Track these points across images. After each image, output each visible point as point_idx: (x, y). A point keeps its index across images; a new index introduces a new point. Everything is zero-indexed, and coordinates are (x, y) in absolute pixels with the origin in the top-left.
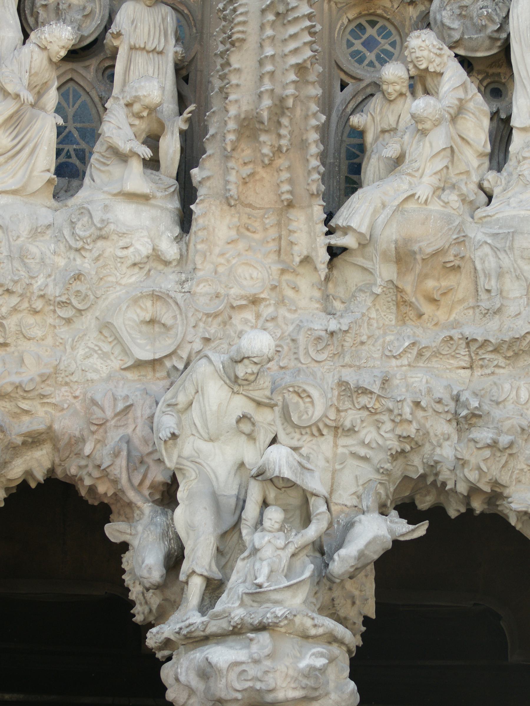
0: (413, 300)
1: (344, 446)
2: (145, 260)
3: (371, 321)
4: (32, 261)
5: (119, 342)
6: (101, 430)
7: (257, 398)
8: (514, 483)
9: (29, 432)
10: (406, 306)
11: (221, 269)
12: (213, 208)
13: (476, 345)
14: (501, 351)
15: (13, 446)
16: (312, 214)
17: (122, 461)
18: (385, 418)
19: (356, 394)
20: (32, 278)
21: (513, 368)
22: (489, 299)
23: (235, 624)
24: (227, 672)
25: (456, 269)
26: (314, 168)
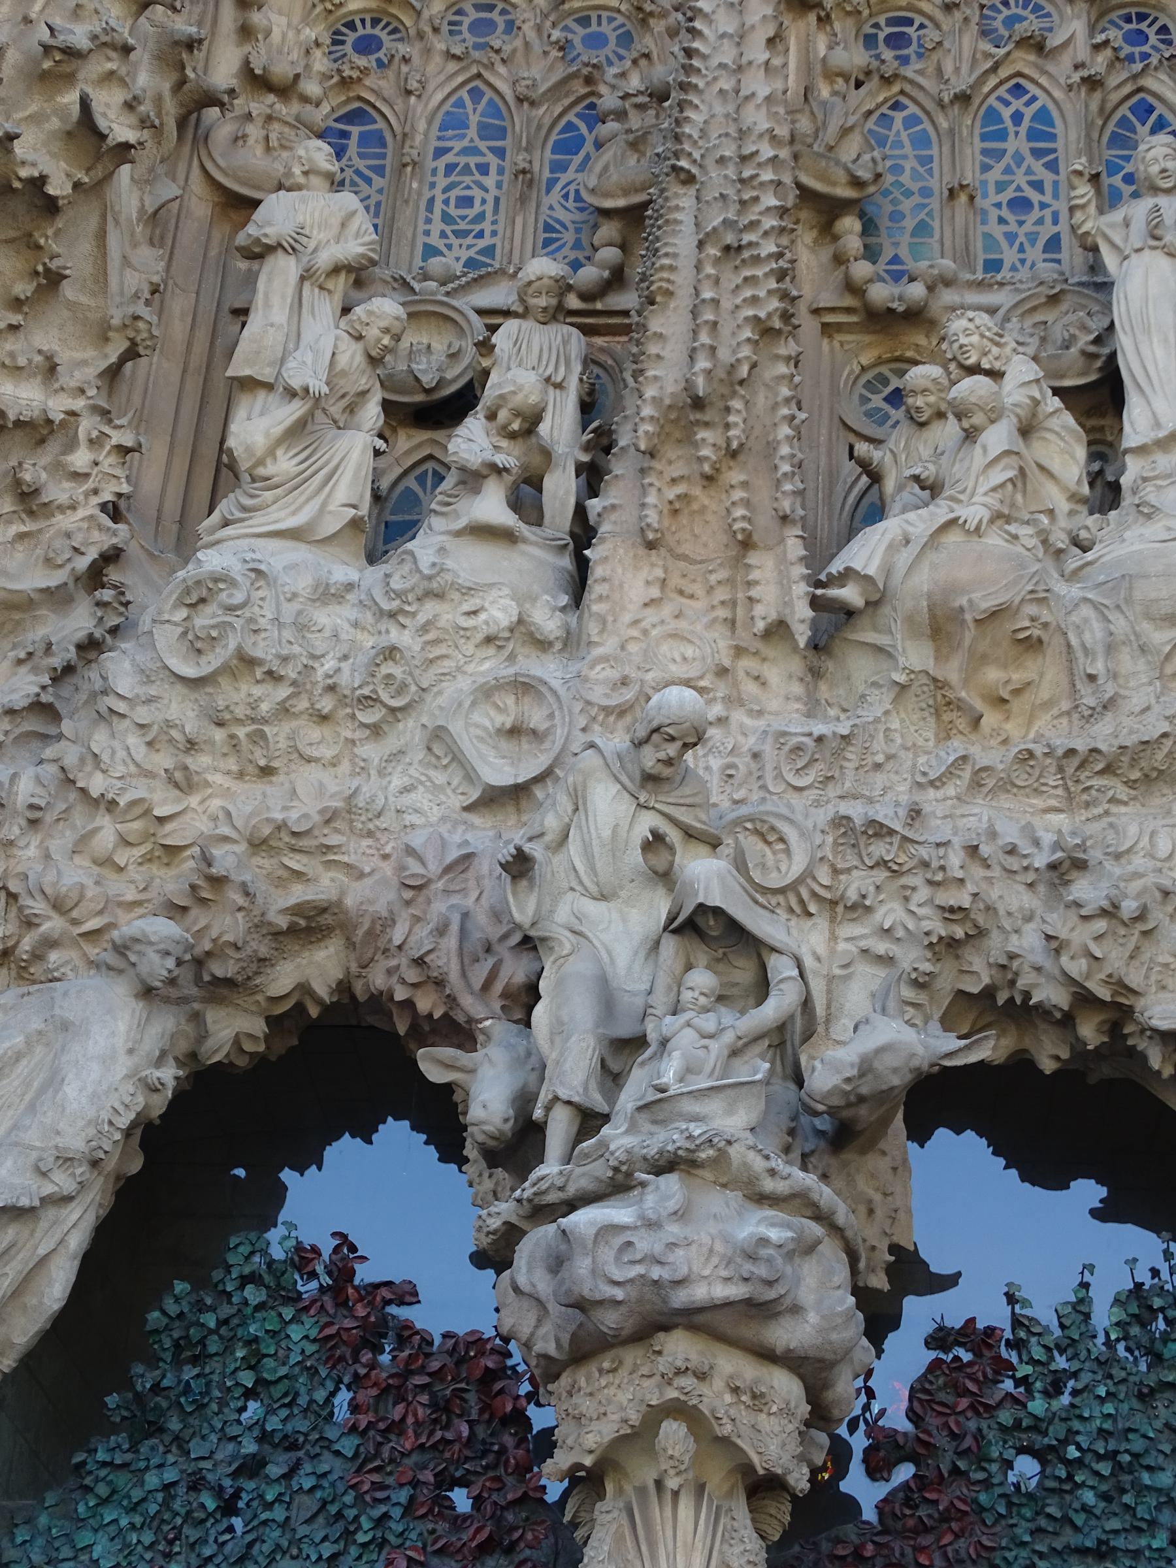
0: (963, 694)
1: (848, 940)
2: (507, 634)
5: (462, 765)
6: (421, 899)
7: (682, 818)
8: (1153, 989)
9: (298, 905)
11: (633, 648)
13: (1075, 762)
15: (273, 930)
16: (785, 552)
17: (451, 942)
20: (314, 657)
23: (615, 1163)
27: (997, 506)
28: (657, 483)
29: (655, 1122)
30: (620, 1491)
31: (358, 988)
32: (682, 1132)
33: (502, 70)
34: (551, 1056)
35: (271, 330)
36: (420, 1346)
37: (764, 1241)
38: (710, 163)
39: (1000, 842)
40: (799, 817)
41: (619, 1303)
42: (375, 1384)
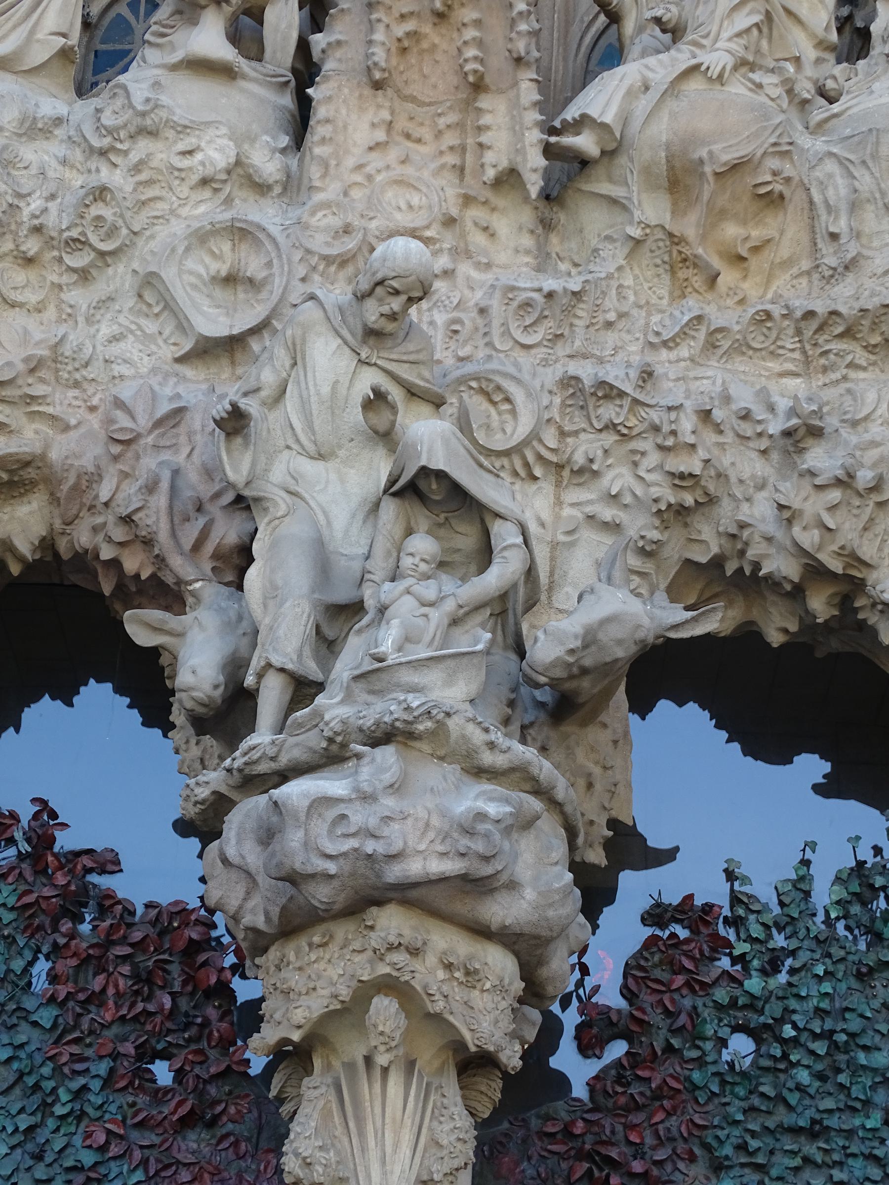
0: (700, 251)
1: (573, 505)
2: (224, 177)
3: (625, 290)
4: (24, 172)
6: (130, 455)
10: (688, 268)
12: (346, 91)
13: (814, 324)
14: (858, 336)
16: (518, 96)
17: (161, 500)
18: (646, 444)
19: (594, 398)
20: (20, 196)
21: (883, 371)
22: (835, 253)
23: (330, 734)
24: (307, 817)
27: (741, 52)
28: (385, 19)
29: (372, 692)
30: (328, 1067)
31: (62, 545)
32: (400, 703)
34: (264, 623)
36: (122, 916)
37: (481, 816)
39: (734, 407)
40: (526, 377)
41: (331, 877)
42: (75, 954)
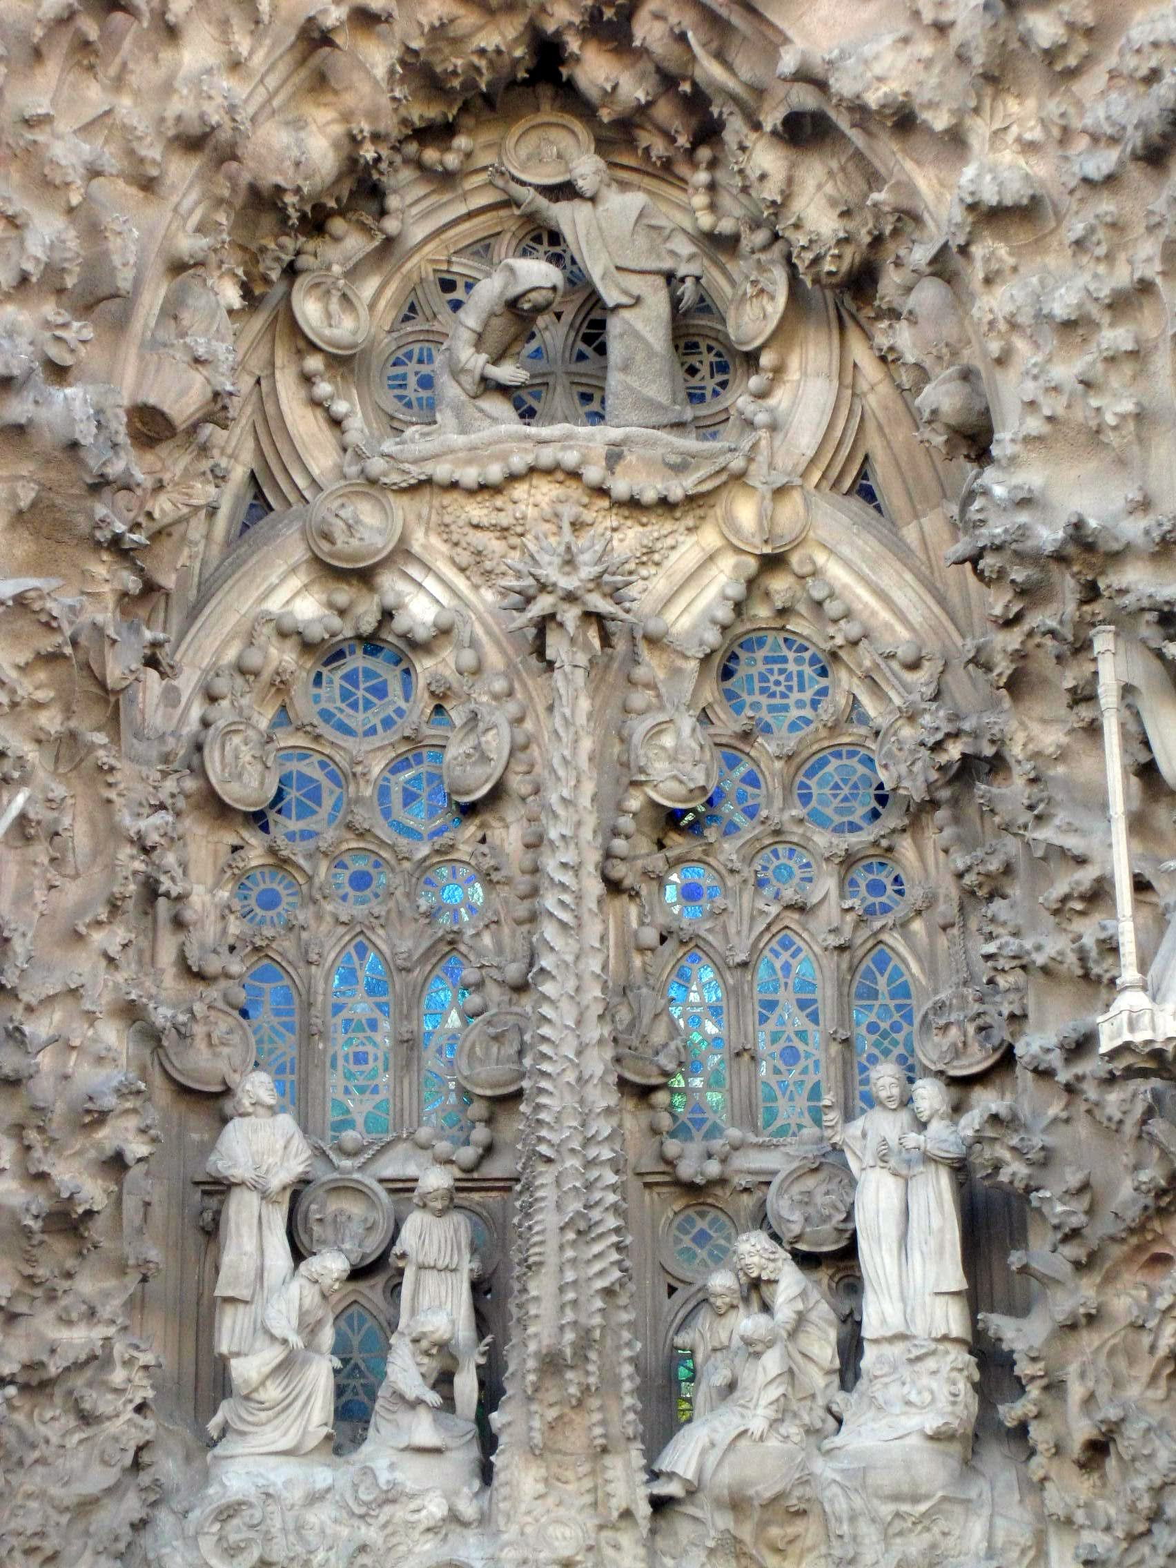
11: (528, 1530)
25: (802, 1513)
26: (629, 1408)
33: (381, 932)
35: (245, 1258)
38: (564, 1150)
